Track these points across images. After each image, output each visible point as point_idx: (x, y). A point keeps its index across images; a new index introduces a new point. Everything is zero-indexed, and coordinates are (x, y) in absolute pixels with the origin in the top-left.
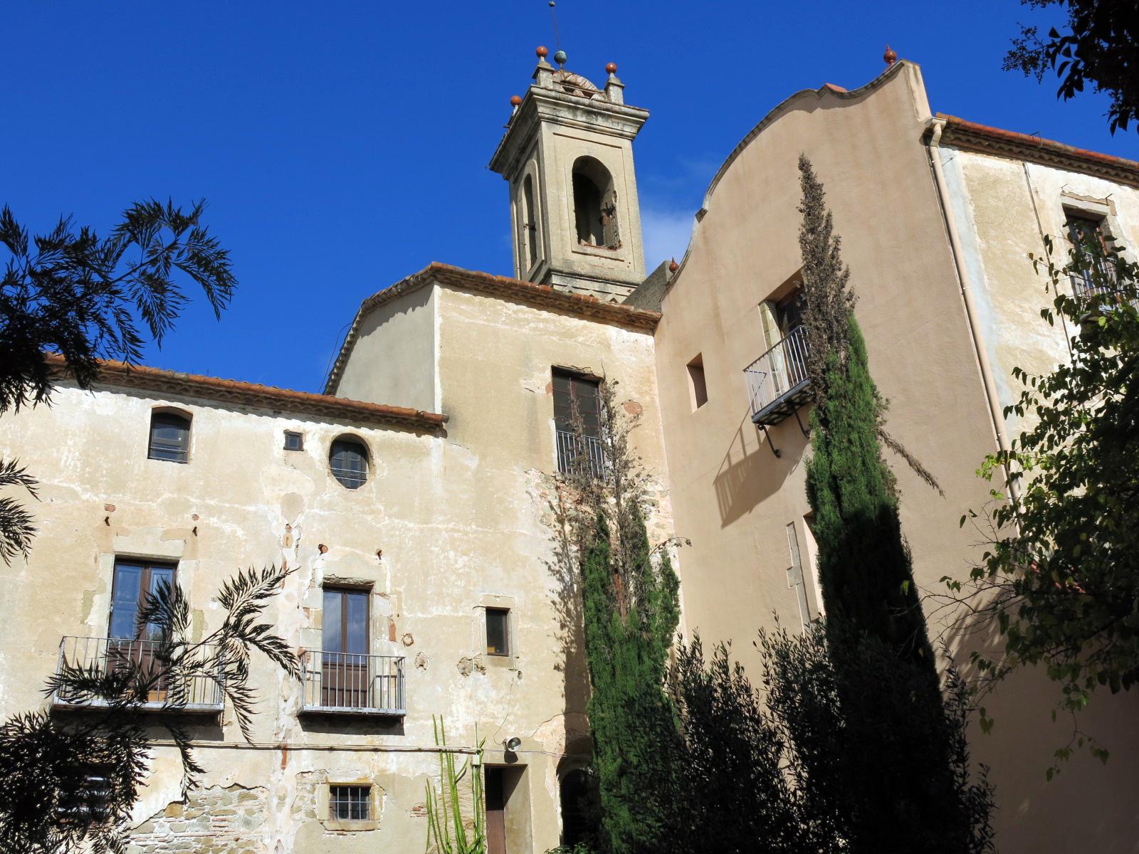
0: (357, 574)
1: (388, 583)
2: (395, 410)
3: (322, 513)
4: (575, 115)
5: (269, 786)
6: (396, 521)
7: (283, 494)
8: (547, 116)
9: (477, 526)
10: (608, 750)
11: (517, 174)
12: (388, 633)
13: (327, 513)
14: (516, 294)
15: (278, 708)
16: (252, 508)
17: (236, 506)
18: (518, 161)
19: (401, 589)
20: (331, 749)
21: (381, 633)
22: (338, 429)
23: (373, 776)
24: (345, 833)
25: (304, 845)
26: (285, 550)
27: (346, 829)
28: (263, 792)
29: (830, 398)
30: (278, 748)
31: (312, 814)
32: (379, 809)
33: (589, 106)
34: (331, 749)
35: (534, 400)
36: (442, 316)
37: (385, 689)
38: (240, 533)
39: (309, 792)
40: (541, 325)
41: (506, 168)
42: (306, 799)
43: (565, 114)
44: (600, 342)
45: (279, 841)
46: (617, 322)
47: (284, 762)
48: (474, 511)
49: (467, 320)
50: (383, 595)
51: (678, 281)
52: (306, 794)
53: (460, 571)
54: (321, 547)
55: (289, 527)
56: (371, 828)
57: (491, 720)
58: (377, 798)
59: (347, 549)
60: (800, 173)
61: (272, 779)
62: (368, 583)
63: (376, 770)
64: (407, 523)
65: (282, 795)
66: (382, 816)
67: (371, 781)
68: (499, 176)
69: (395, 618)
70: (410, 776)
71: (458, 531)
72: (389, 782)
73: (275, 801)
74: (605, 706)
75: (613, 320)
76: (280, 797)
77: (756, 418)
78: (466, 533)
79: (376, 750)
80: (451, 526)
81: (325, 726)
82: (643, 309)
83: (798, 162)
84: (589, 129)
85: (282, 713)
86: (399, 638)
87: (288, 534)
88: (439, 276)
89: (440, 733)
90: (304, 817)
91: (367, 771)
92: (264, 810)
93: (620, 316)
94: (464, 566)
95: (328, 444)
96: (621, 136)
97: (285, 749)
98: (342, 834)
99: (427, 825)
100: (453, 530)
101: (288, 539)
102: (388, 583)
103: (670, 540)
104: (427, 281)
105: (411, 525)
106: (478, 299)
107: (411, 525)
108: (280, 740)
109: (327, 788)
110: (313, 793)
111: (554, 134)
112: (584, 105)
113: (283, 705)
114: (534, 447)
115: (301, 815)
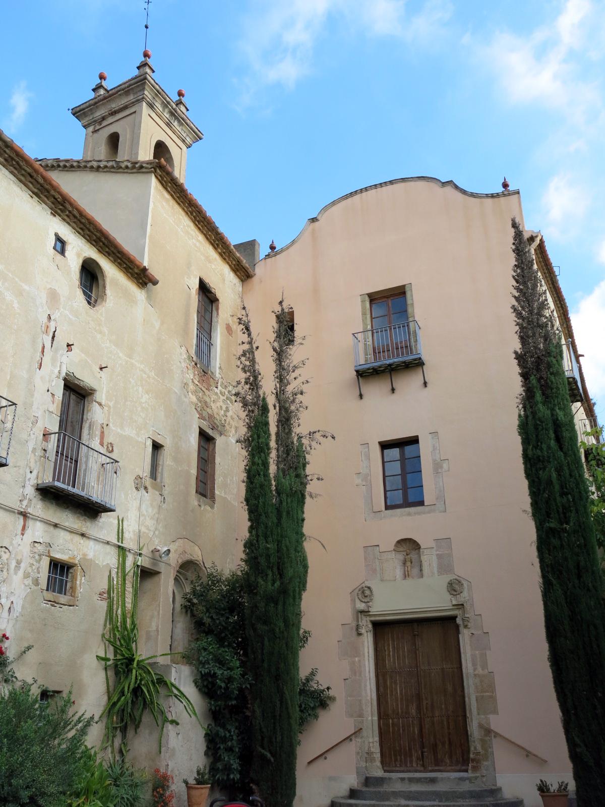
0: (87, 378)
1: (104, 397)
2: (132, 257)
3: (71, 317)
4: (164, 110)
5: (11, 548)
6: (113, 347)
7: (49, 286)
8: (148, 100)
9: (155, 374)
10: (270, 573)
11: (98, 127)
12: (99, 437)
13: (74, 319)
14: (192, 214)
15: (26, 477)
16: (26, 287)
17: (17, 279)
18: (104, 118)
19: (111, 404)
20: (56, 526)
21: (95, 436)
22: (92, 253)
23: (78, 558)
24: (56, 605)
25: (29, 610)
26: (45, 336)
27: (57, 602)
28: (5, 552)
29: (551, 374)
30: (21, 513)
31: (36, 582)
32: (79, 588)
33: (174, 109)
34: (56, 526)
35: (189, 296)
36: (153, 202)
37: (109, 482)
38: (16, 305)
39: (37, 561)
40: (198, 244)
41: (87, 119)
42: (34, 567)
43: (158, 106)
44: (220, 275)
45: (12, 602)
46: (230, 266)
47: (24, 528)
48: (154, 362)
49: (165, 215)
50: (100, 404)
51: (278, 256)
52: (35, 563)
53: (144, 405)
54: (68, 345)
55: (49, 317)
56: (72, 604)
57: (147, 531)
58: (79, 577)
59: (83, 355)
60: (513, 230)
61: (14, 542)
62: (91, 390)
63: (81, 554)
64: (119, 352)
65: (19, 559)
66: (80, 595)
67: (77, 562)
68: (77, 124)
69: (105, 426)
70: (100, 564)
71: (145, 374)
72: (88, 565)
73: (13, 564)
74: (270, 539)
75: (228, 263)
76: (18, 560)
77: (359, 368)
78: (149, 377)
79: (83, 535)
80: (142, 366)
81: (52, 504)
82: (249, 265)
83: (511, 222)
84: (168, 125)
85: (27, 482)
86: (105, 444)
87: (48, 324)
88: (158, 171)
89: (120, 534)
90: (31, 584)
91: (75, 553)
92: (5, 570)
93: (234, 263)
94: (146, 402)
95: (81, 262)
96: (183, 141)
97: (24, 515)
98: (52, 605)
99: (105, 608)
100: (142, 370)
101: (48, 327)
102: (104, 397)
103: (319, 431)
104: (144, 170)
105: (121, 355)
106: (172, 202)
107: (121, 355)
108: (23, 507)
109: (48, 560)
110: (39, 563)
111: (149, 115)
112: (172, 107)
113: (29, 475)
114: (186, 331)
115: (29, 581)
